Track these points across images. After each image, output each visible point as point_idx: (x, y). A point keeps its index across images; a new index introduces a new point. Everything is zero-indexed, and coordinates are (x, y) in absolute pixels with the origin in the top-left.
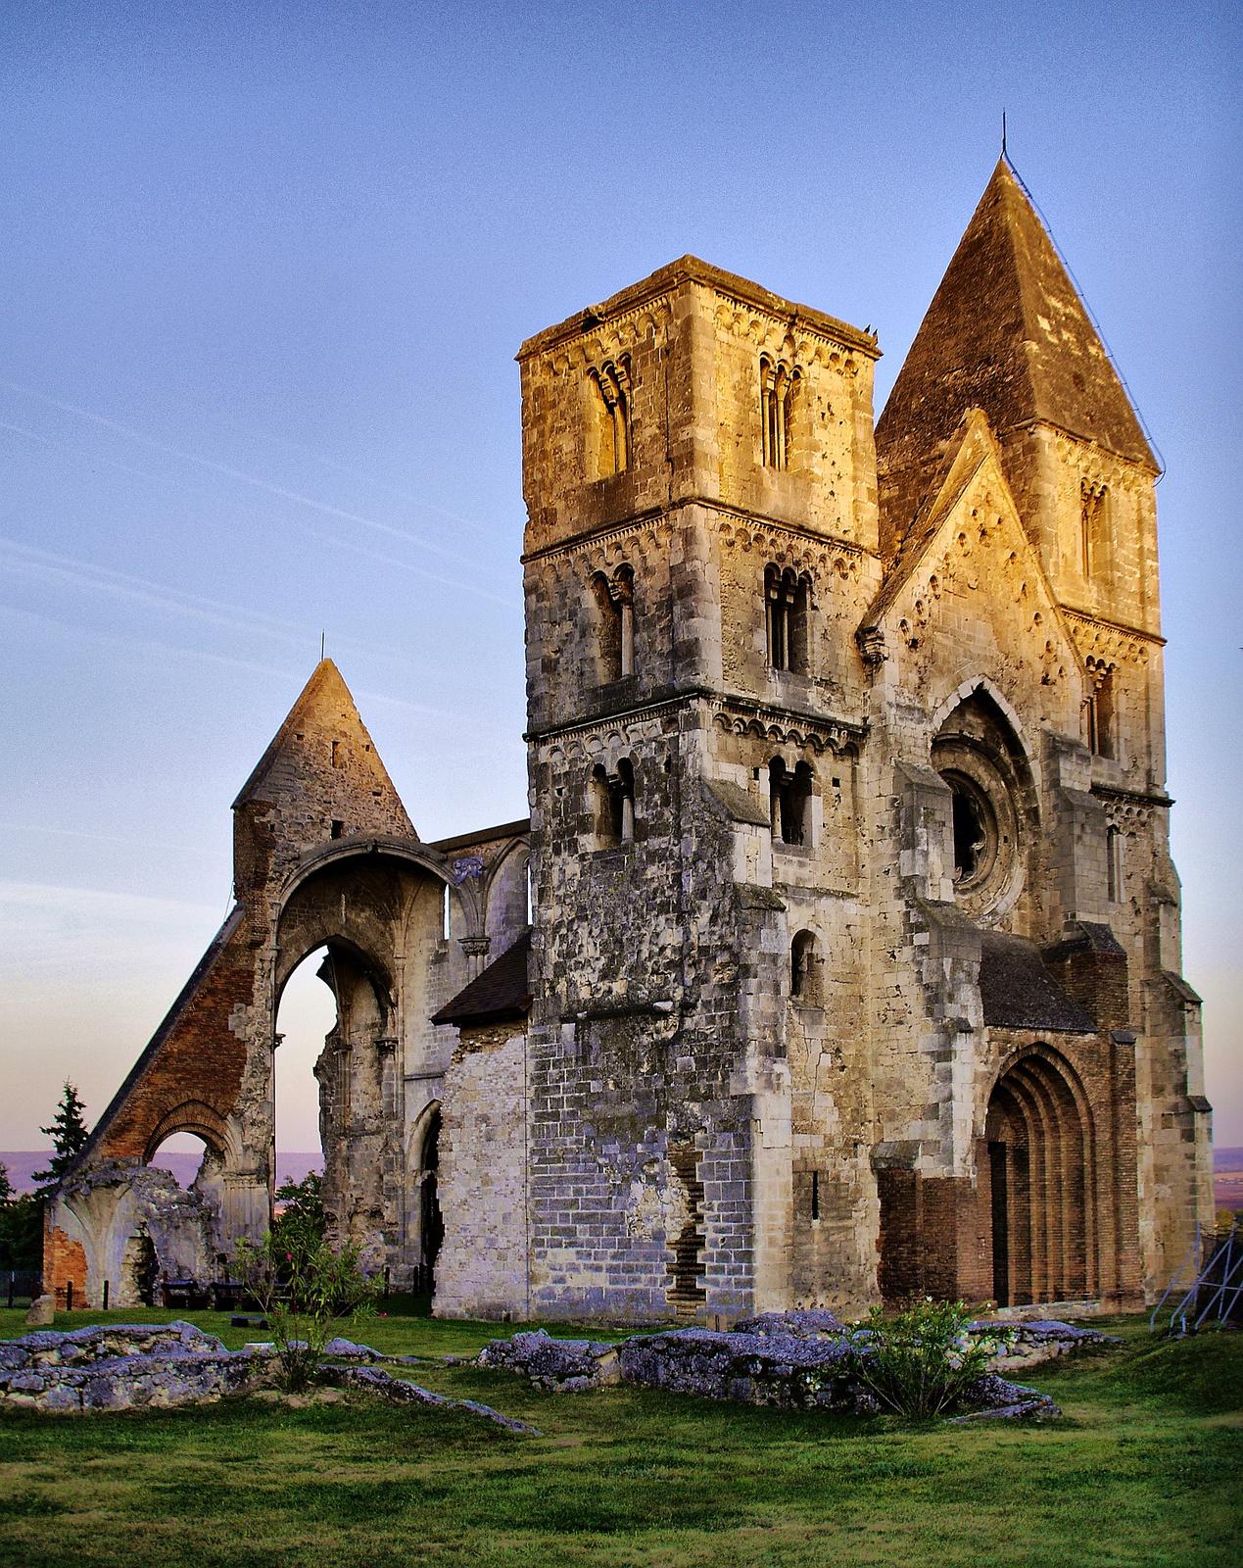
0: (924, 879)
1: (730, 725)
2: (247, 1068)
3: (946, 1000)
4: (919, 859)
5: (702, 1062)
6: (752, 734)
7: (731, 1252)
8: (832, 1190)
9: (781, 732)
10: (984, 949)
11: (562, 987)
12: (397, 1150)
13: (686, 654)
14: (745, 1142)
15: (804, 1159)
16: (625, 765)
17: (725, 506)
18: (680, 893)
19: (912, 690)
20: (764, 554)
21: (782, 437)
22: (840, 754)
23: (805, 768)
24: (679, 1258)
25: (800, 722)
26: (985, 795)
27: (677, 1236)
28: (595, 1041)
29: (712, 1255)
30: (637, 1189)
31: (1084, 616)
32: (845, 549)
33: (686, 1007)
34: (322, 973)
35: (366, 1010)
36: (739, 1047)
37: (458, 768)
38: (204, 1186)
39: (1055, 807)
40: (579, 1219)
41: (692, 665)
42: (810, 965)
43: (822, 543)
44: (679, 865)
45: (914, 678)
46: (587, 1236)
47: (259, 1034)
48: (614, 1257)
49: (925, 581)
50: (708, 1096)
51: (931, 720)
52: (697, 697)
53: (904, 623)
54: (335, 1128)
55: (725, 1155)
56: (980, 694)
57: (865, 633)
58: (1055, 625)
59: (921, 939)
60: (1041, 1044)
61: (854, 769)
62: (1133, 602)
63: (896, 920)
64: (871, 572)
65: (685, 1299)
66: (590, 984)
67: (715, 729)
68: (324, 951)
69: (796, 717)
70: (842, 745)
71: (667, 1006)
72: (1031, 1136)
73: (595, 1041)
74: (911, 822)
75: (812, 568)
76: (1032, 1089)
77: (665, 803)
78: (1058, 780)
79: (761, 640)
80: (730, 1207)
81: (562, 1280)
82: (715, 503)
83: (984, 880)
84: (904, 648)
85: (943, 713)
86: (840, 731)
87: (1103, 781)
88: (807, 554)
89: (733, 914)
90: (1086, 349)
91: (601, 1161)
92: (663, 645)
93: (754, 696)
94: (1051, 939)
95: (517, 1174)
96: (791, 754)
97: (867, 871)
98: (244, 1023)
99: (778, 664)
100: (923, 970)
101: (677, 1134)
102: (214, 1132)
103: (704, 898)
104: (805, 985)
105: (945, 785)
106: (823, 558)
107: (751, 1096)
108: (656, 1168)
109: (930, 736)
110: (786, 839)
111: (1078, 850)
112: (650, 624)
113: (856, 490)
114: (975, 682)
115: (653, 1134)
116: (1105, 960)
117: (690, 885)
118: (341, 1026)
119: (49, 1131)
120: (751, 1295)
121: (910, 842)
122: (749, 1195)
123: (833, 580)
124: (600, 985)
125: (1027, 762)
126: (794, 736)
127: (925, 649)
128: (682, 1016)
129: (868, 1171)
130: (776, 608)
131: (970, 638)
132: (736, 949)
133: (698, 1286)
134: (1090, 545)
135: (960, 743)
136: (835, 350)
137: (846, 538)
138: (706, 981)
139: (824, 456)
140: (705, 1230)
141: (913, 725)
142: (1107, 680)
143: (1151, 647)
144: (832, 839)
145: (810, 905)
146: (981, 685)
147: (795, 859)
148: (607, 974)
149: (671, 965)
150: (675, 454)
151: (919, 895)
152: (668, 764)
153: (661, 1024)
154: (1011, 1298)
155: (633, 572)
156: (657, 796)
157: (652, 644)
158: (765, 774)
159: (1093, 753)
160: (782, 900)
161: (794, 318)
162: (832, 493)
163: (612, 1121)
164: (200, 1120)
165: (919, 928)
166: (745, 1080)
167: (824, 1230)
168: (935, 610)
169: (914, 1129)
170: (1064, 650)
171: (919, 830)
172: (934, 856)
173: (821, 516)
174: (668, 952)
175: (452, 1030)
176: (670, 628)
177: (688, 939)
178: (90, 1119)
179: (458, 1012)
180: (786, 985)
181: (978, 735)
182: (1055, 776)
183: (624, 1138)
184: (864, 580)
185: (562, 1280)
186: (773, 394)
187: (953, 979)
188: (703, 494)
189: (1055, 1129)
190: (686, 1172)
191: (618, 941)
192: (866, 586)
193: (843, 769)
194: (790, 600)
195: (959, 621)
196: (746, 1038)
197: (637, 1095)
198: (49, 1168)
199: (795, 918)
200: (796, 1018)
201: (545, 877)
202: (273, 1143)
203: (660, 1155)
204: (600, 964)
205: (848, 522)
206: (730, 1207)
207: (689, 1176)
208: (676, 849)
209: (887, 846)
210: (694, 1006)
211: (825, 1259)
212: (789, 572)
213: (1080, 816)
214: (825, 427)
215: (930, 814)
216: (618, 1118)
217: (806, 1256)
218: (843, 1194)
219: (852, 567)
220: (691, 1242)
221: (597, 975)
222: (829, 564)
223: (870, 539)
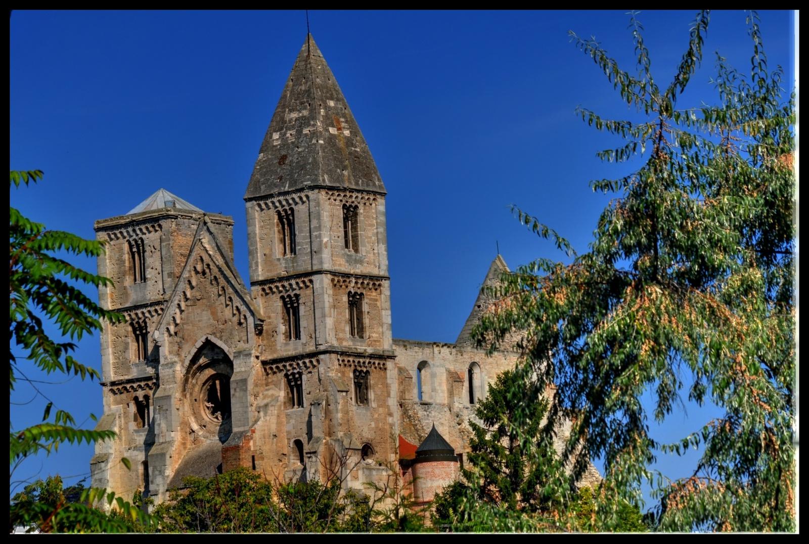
0: (159, 435)
45: (176, 348)
56: (208, 343)
67: (111, 394)
96: (140, 394)
114: (203, 339)
127: (180, 334)
131: (199, 321)
146: (207, 339)
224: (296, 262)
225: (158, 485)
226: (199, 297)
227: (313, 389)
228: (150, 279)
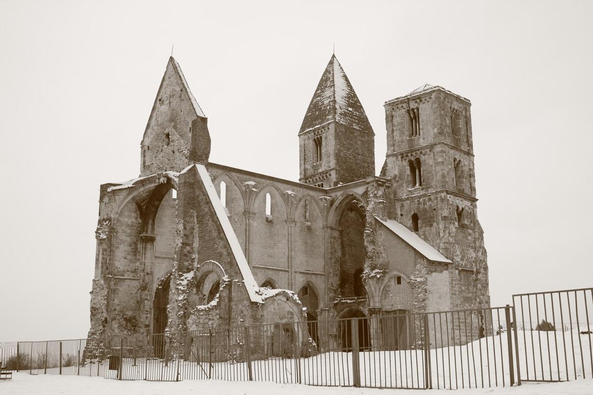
28: (462, 277)
33: (478, 272)
50: (483, 295)
73: (462, 277)
124: (461, 262)
148: (462, 260)
204: (460, 257)
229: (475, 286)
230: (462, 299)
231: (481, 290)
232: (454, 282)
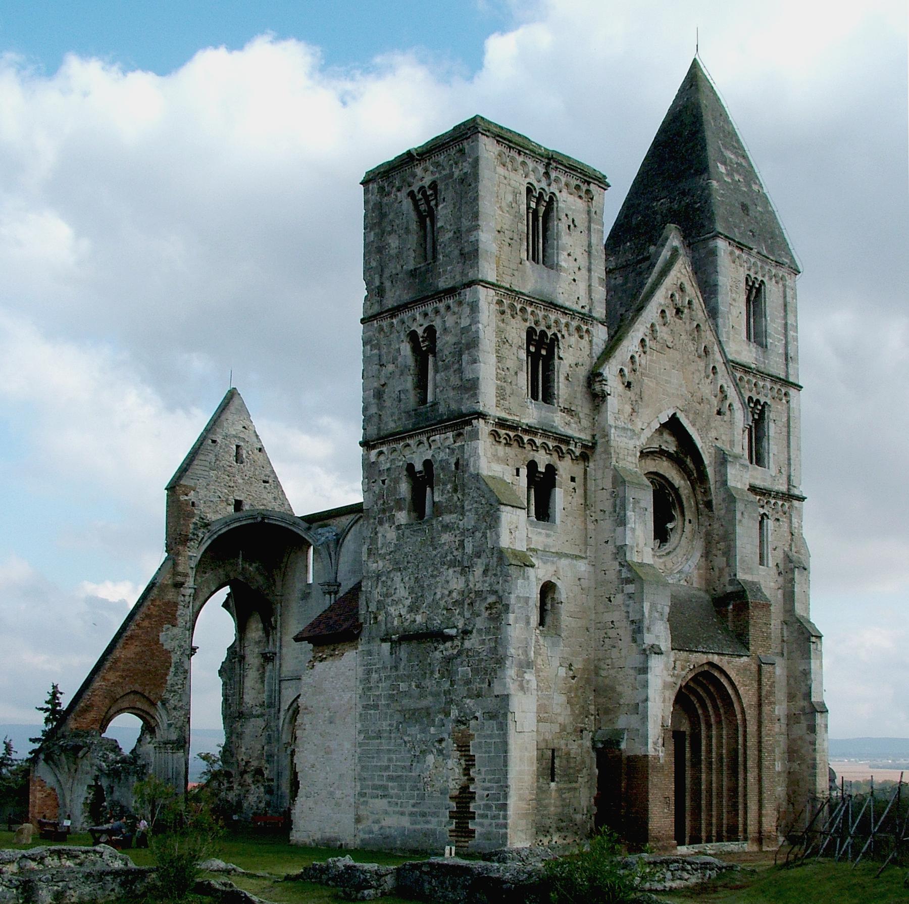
1: (500, 438)
2: (172, 669)
3: (645, 630)
4: (629, 533)
5: (476, 671)
6: (515, 444)
7: (493, 803)
8: (564, 762)
9: (535, 443)
10: (673, 597)
11: (380, 618)
12: (274, 729)
13: (471, 387)
14: (503, 727)
15: (545, 741)
16: (428, 464)
17: (499, 287)
18: (463, 554)
19: (626, 415)
20: (525, 320)
21: (541, 241)
22: (575, 459)
23: (551, 470)
24: (457, 807)
25: (549, 437)
26: (676, 490)
27: (456, 793)
29: (479, 807)
30: (430, 759)
31: (746, 369)
32: (582, 319)
33: (466, 633)
34: (226, 605)
35: (255, 632)
36: (500, 662)
37: (316, 467)
38: (141, 750)
39: (724, 500)
40: (390, 778)
41: (475, 395)
42: (552, 606)
43: (566, 314)
44: (462, 534)
45: (628, 409)
46: (396, 791)
47: (181, 647)
48: (413, 806)
49: (637, 342)
51: (639, 438)
52: (477, 418)
53: (621, 370)
54: (234, 714)
55: (490, 736)
57: (594, 376)
58: (726, 374)
59: (630, 588)
60: (711, 664)
61: (586, 470)
62: (782, 360)
63: (612, 575)
64: (601, 334)
65: (462, 836)
66: (401, 616)
67: (490, 440)
68: (227, 589)
69: (546, 433)
70: (578, 454)
71: (453, 632)
72: (703, 727)
74: (624, 507)
75: (559, 331)
76: (703, 695)
77: (455, 490)
78: (726, 481)
79: (523, 380)
80: (493, 772)
81: (377, 822)
82: (493, 285)
83: (674, 549)
84: (621, 388)
85: (648, 433)
86: (576, 443)
87: (759, 483)
88: (556, 322)
89: (499, 569)
90: (751, 187)
91: (406, 739)
92: (455, 380)
93: (517, 419)
94: (719, 590)
95: (349, 747)
96: (543, 460)
97: (592, 542)
98: (168, 638)
99: (534, 396)
100: (630, 610)
101: (459, 722)
102: (148, 713)
103: (479, 557)
104: (549, 619)
105: (648, 483)
106: (567, 325)
107: (508, 696)
108: (444, 745)
109: (639, 449)
110: (538, 518)
111: (739, 529)
112: (447, 368)
113: (590, 278)
115: (442, 720)
116: (756, 606)
117: (469, 549)
118: (238, 643)
119: (41, 709)
120: (506, 833)
121: (622, 522)
122: (506, 764)
123: (573, 339)
124: (408, 616)
125: (705, 468)
126: (545, 446)
127: (635, 388)
128: (463, 639)
129: (591, 750)
130: (534, 358)
131: (667, 382)
132: (501, 593)
133: (470, 827)
134: (752, 320)
135: (662, 453)
136: (578, 182)
137: (583, 311)
138: (479, 615)
139: (569, 255)
140: (475, 788)
141: (626, 440)
142: (762, 413)
143: (792, 392)
144: (570, 518)
145: (553, 563)
146: (675, 414)
147: (543, 531)
148: (413, 609)
149: (454, 603)
150: (466, 250)
151: (628, 559)
152: (457, 464)
153: (448, 644)
154: (687, 840)
155: (435, 332)
156: (449, 486)
157: (448, 381)
158: (524, 472)
159: (751, 463)
160: (533, 560)
161: (552, 161)
162: (574, 280)
163: (415, 710)
164: (139, 705)
165: (628, 581)
166: (505, 685)
167: (559, 790)
168: (643, 362)
169: (622, 721)
170: (731, 392)
171: (629, 513)
172: (639, 532)
173: (566, 295)
174: (454, 595)
175: (308, 646)
176: (460, 371)
177: (468, 585)
178: (65, 702)
179: (311, 634)
180: (535, 618)
181: (672, 449)
182: (724, 478)
183: (422, 723)
184: (595, 340)
185: (377, 822)
186: (535, 212)
187: (650, 617)
188: (484, 279)
189: (719, 722)
190: (463, 748)
191: (422, 587)
192: (597, 344)
193: (577, 469)
194: (544, 352)
195: (660, 369)
196: (506, 656)
197: (431, 693)
198: (39, 735)
199: (541, 572)
200: (541, 641)
201: (374, 540)
202: (189, 722)
203: (446, 736)
204: (408, 602)
205: (584, 301)
206: (493, 772)
207: (465, 751)
208: (461, 523)
209: (607, 524)
210: (471, 632)
211: (559, 810)
212: (543, 333)
213: (740, 506)
214: (570, 235)
215: (636, 501)
216: (418, 709)
217: (546, 807)
218: (572, 765)
219: (587, 331)
220: (465, 797)
221: (406, 609)
222: (572, 329)
223: (600, 311)
224: (768, 359)
225: (657, 637)
226: (670, 345)
227: (780, 544)
228: (566, 270)
229: (448, 671)
230: (397, 717)
231: (468, 682)
232: (375, 676)
